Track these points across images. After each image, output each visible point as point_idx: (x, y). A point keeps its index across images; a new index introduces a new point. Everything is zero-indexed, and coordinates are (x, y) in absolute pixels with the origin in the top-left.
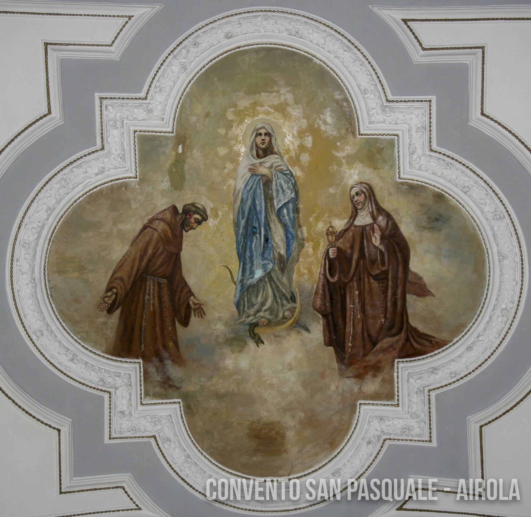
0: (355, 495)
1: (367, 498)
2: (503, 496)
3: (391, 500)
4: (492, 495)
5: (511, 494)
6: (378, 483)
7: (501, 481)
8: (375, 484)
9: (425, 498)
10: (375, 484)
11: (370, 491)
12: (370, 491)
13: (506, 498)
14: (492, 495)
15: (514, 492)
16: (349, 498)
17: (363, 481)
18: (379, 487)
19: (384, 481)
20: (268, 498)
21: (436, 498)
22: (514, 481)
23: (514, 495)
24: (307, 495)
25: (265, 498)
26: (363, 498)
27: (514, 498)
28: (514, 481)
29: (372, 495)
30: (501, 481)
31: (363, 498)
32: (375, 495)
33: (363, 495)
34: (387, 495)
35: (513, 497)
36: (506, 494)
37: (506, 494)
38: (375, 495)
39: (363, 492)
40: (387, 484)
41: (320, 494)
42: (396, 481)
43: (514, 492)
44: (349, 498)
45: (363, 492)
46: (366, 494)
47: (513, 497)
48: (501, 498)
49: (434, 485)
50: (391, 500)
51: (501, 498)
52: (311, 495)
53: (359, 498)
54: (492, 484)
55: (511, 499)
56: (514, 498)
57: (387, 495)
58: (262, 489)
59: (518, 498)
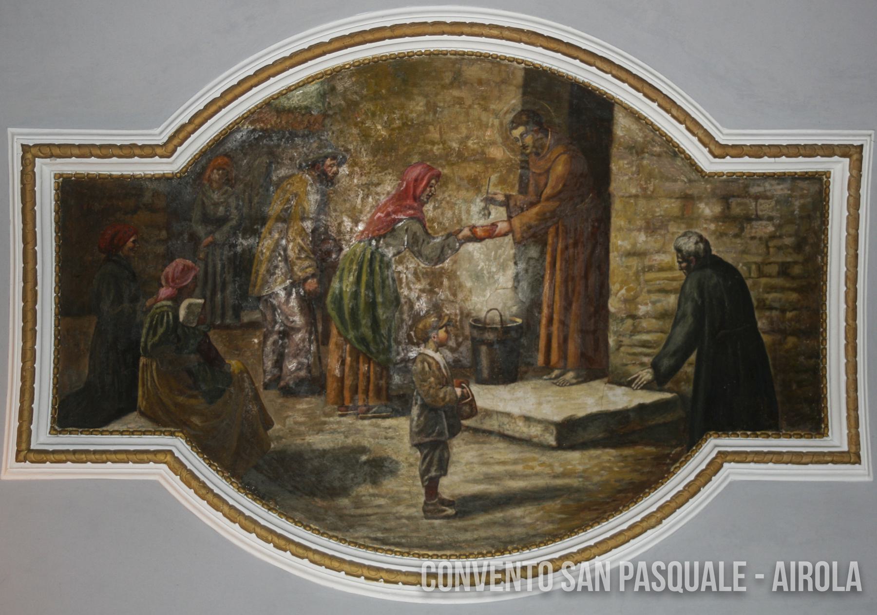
0: (630, 583)
1: (647, 589)
2: (838, 586)
3: (681, 591)
4: (822, 584)
5: (850, 583)
6: (663, 567)
7: (835, 564)
8: (659, 568)
9: (729, 589)
10: (659, 568)
11: (652, 578)
12: (652, 578)
13: (842, 589)
14: (822, 584)
15: (854, 580)
16: (622, 589)
17: (642, 565)
18: (664, 573)
19: (671, 565)
20: (508, 589)
21: (744, 589)
22: (854, 565)
23: (854, 584)
25: (504, 588)
26: (642, 588)
27: (854, 588)
28: (854, 565)
29: (654, 584)
30: (835, 564)
31: (642, 588)
32: (659, 585)
33: (642, 584)
34: (675, 584)
35: (778, 587)
36: (842, 582)
37: (842, 582)
38: (659, 585)
39: (642, 580)
40: (675, 569)
42: (687, 564)
43: (854, 580)
44: (622, 589)
45: (642, 580)
46: (646, 583)
47: (778, 587)
48: (836, 588)
49: (741, 570)
50: (681, 591)
51: (836, 588)
53: (636, 589)
54: (822, 569)
55: (848, 589)
56: (854, 588)
57: (675, 584)
58: (499, 576)
59: (859, 589)
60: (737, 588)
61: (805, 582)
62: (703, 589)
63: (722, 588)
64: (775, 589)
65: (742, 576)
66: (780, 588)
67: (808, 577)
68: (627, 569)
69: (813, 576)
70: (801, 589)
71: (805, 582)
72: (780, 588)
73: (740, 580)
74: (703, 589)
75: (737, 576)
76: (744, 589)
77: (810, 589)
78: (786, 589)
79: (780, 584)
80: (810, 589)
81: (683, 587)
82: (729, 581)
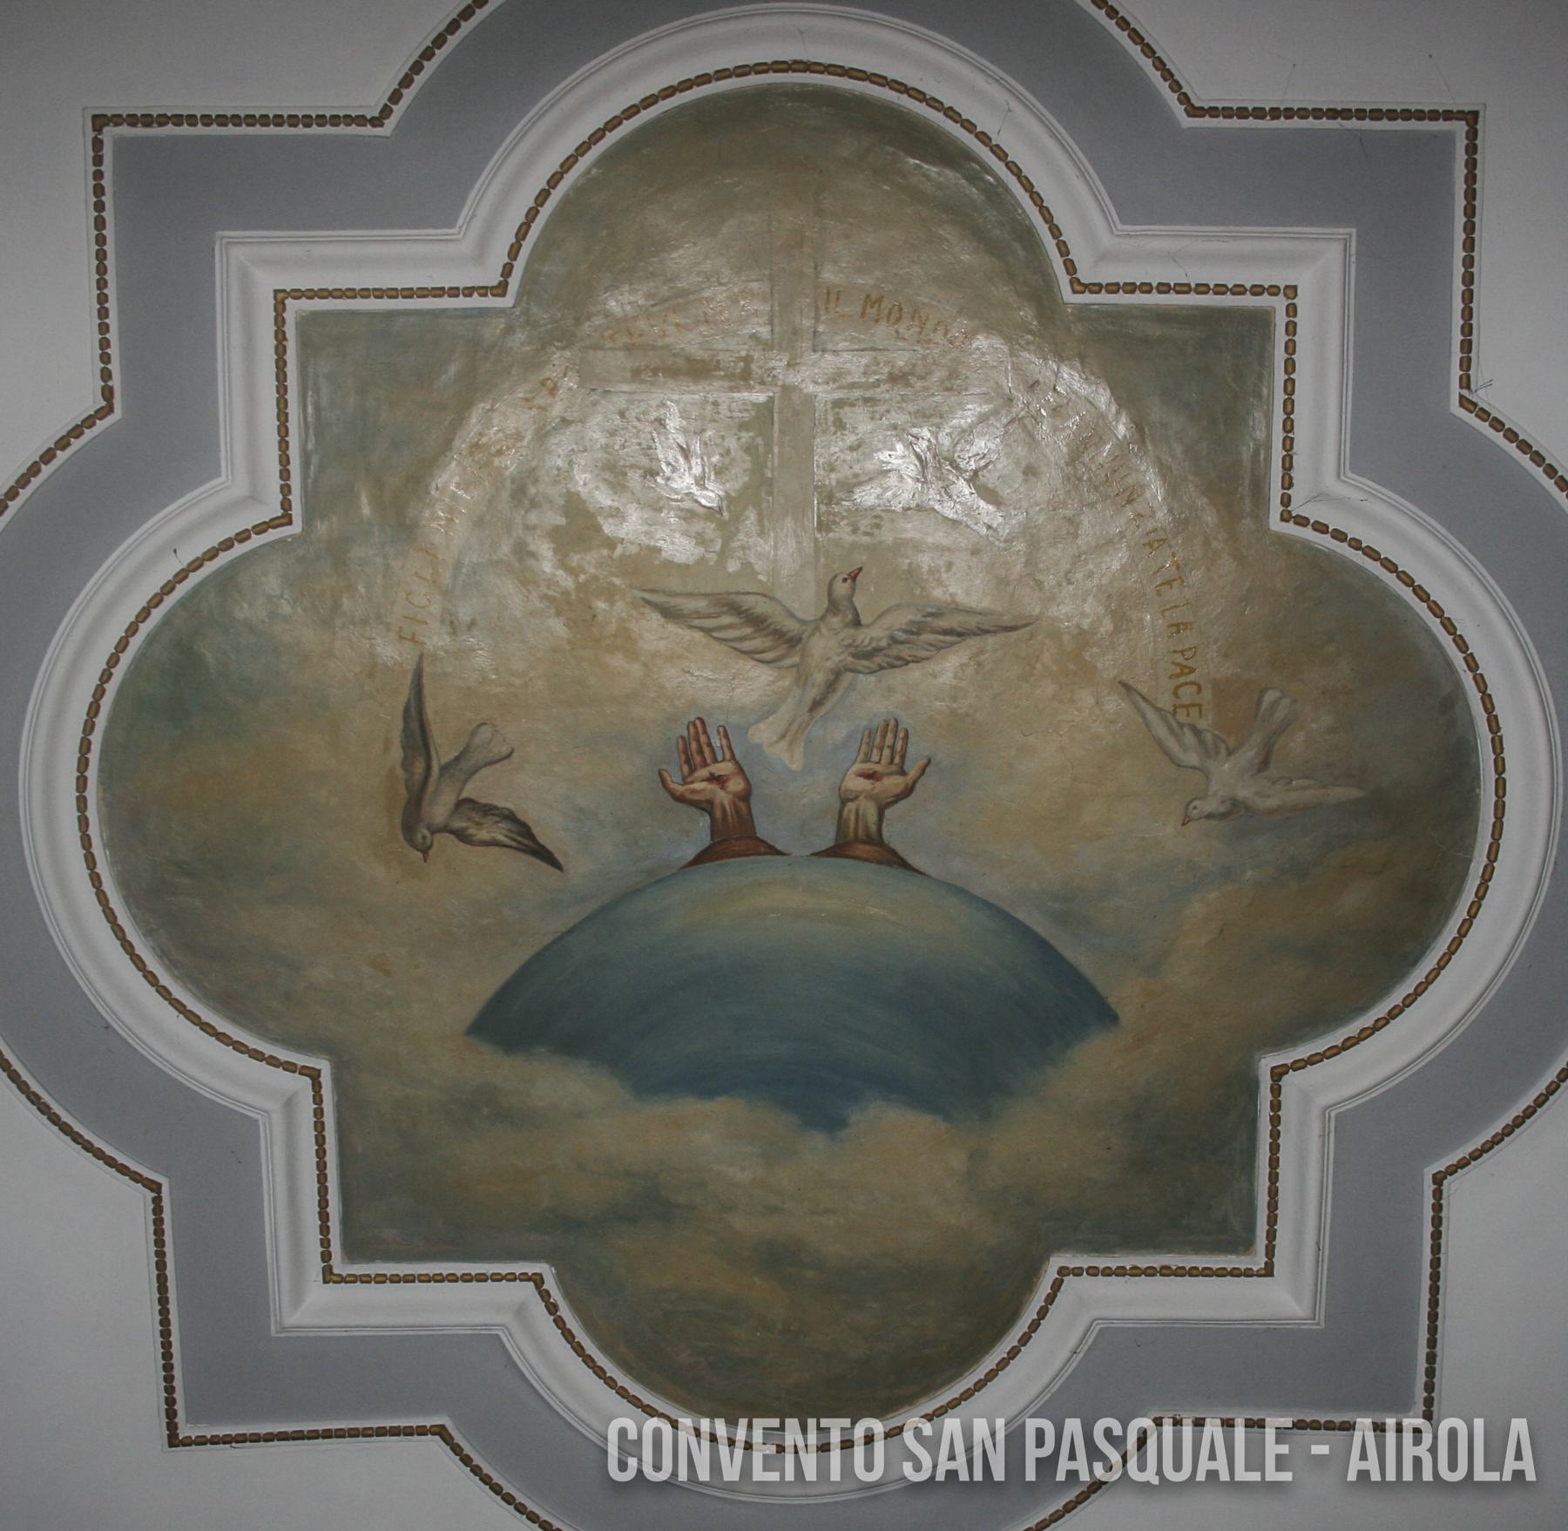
3: (1155, 1481)
4: (1453, 1466)
5: (1510, 1465)
7: (1479, 1424)
9: (1255, 1476)
13: (1493, 1476)
21: (1287, 1476)
24: (908, 1468)
25: (782, 1476)
30: (1479, 1424)
41: (944, 1466)
48: (1480, 1475)
50: (1155, 1481)
52: (918, 1468)
55: (1507, 1477)
56: (1519, 1475)
59: (1531, 1476)
60: (1272, 1475)
61: (1417, 1461)
62: (1201, 1477)
63: (1242, 1475)
64: (1352, 1476)
65: (1284, 1449)
66: (1364, 1475)
67: (1422, 1451)
68: (1040, 1434)
69: (1433, 1450)
70: (1408, 1476)
71: (1417, 1461)
72: (1364, 1475)
73: (1279, 1457)
74: (1201, 1477)
75: (1272, 1449)
76: (1287, 1476)
77: (1427, 1476)
78: (1375, 1476)
79: (1364, 1466)
80: (1427, 1476)
81: (1160, 1472)
82: (1255, 1460)
